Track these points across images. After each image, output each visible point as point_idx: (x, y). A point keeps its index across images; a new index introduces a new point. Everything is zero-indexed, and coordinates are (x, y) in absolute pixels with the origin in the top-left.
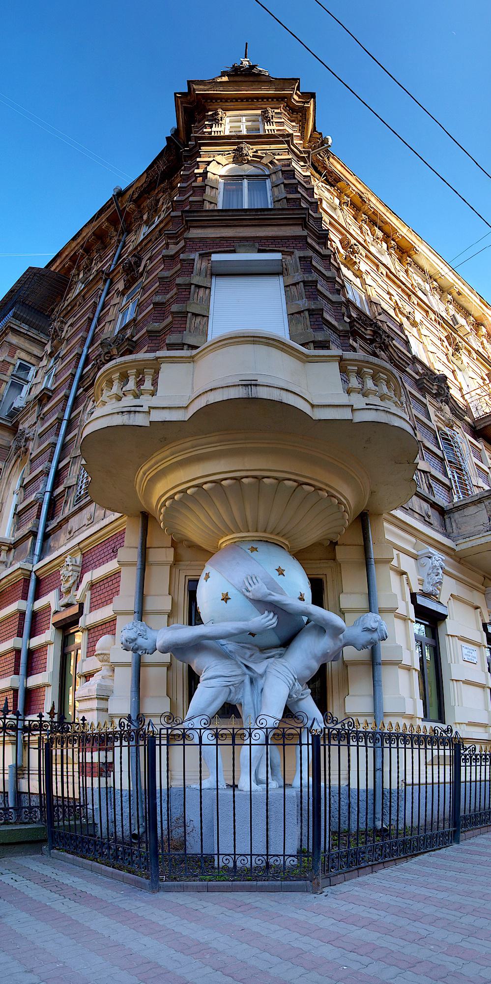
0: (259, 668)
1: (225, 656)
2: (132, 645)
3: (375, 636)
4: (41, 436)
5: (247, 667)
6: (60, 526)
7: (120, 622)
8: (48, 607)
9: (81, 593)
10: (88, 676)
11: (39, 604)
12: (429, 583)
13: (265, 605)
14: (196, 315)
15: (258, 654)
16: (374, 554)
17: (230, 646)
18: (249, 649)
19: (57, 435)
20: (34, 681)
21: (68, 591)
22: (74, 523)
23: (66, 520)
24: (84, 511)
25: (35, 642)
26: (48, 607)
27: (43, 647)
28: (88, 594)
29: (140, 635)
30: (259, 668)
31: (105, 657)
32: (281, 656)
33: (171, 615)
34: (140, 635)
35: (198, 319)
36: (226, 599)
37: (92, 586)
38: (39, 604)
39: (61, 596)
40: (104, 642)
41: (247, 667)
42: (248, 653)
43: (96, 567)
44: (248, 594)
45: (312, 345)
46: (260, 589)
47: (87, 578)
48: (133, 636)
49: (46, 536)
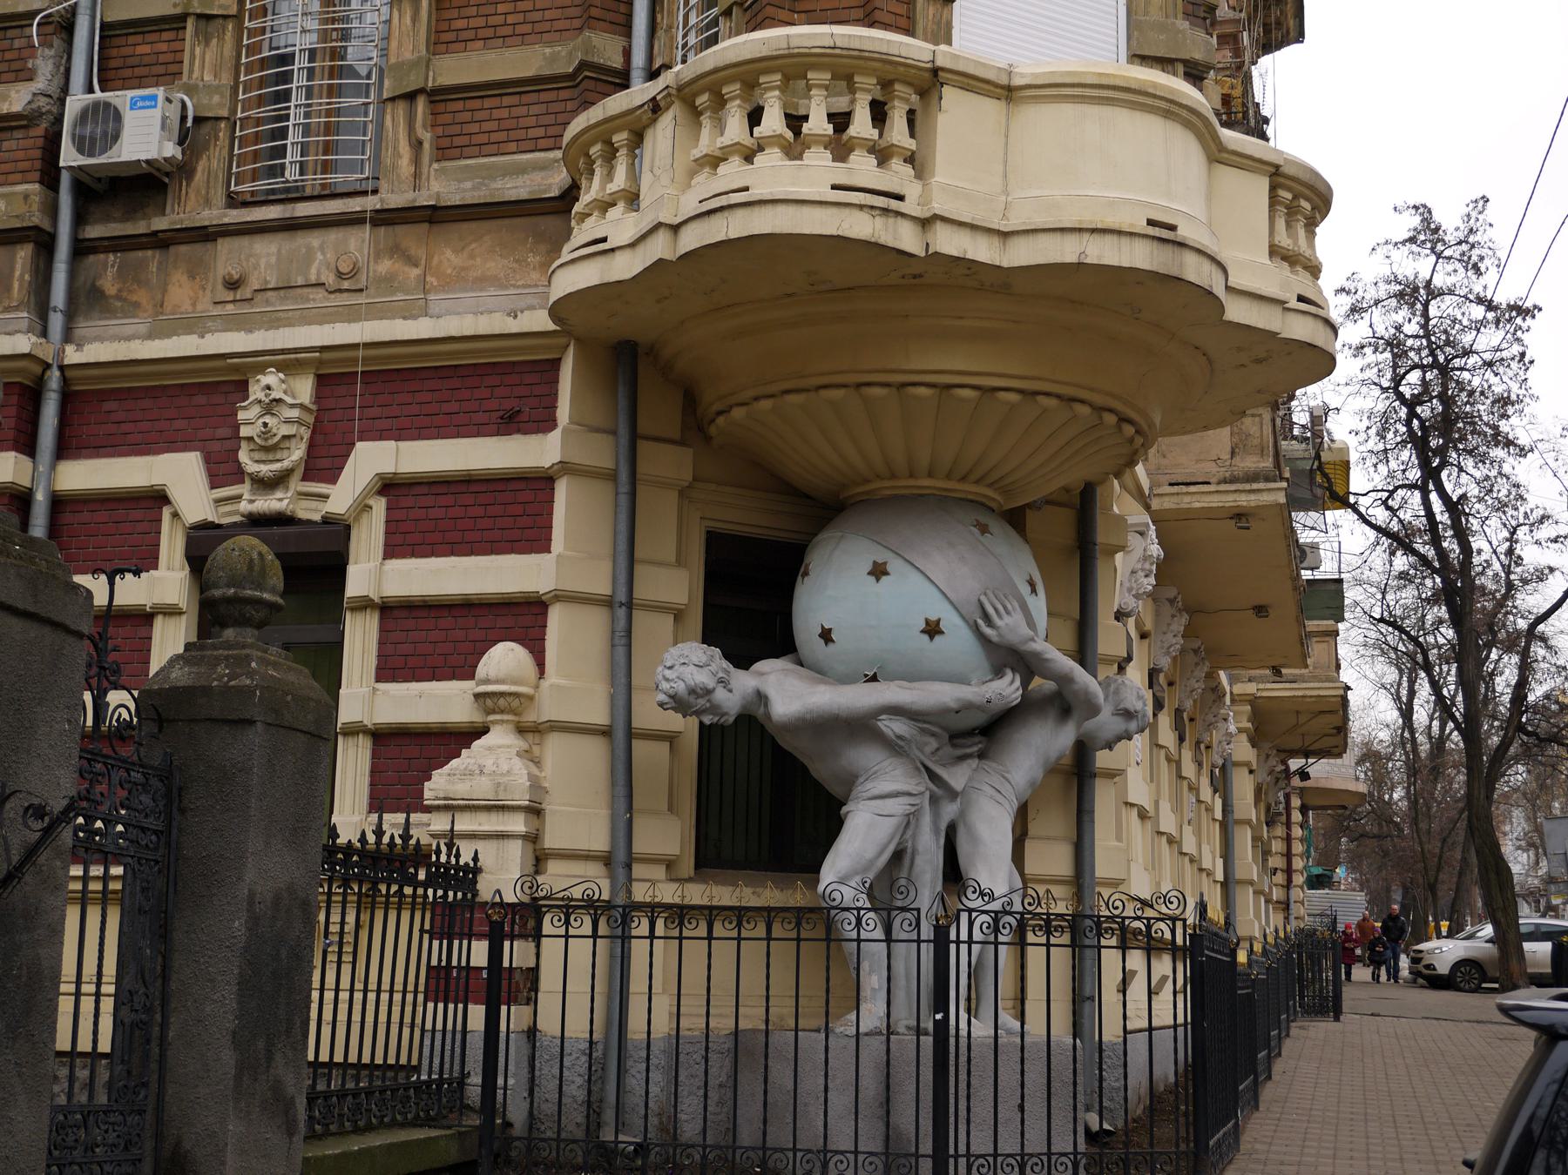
0: (957, 777)
1: (895, 747)
2: (701, 702)
3: (1133, 726)
5: (933, 776)
6: (161, 241)
7: (557, 620)
9: (340, 497)
12: (1130, 590)
13: (1008, 658)
15: (948, 750)
16: (1102, 537)
17: (894, 727)
18: (933, 735)
22: (263, 258)
24: (314, 239)
28: (379, 506)
29: (720, 681)
30: (957, 777)
31: (515, 703)
32: (982, 756)
33: (679, 615)
34: (720, 681)
36: (933, 629)
37: (389, 486)
40: (504, 660)
41: (933, 776)
42: (933, 744)
43: (400, 434)
44: (988, 631)
45: (1180, 68)
46: (1011, 626)
47: (372, 459)
48: (711, 683)
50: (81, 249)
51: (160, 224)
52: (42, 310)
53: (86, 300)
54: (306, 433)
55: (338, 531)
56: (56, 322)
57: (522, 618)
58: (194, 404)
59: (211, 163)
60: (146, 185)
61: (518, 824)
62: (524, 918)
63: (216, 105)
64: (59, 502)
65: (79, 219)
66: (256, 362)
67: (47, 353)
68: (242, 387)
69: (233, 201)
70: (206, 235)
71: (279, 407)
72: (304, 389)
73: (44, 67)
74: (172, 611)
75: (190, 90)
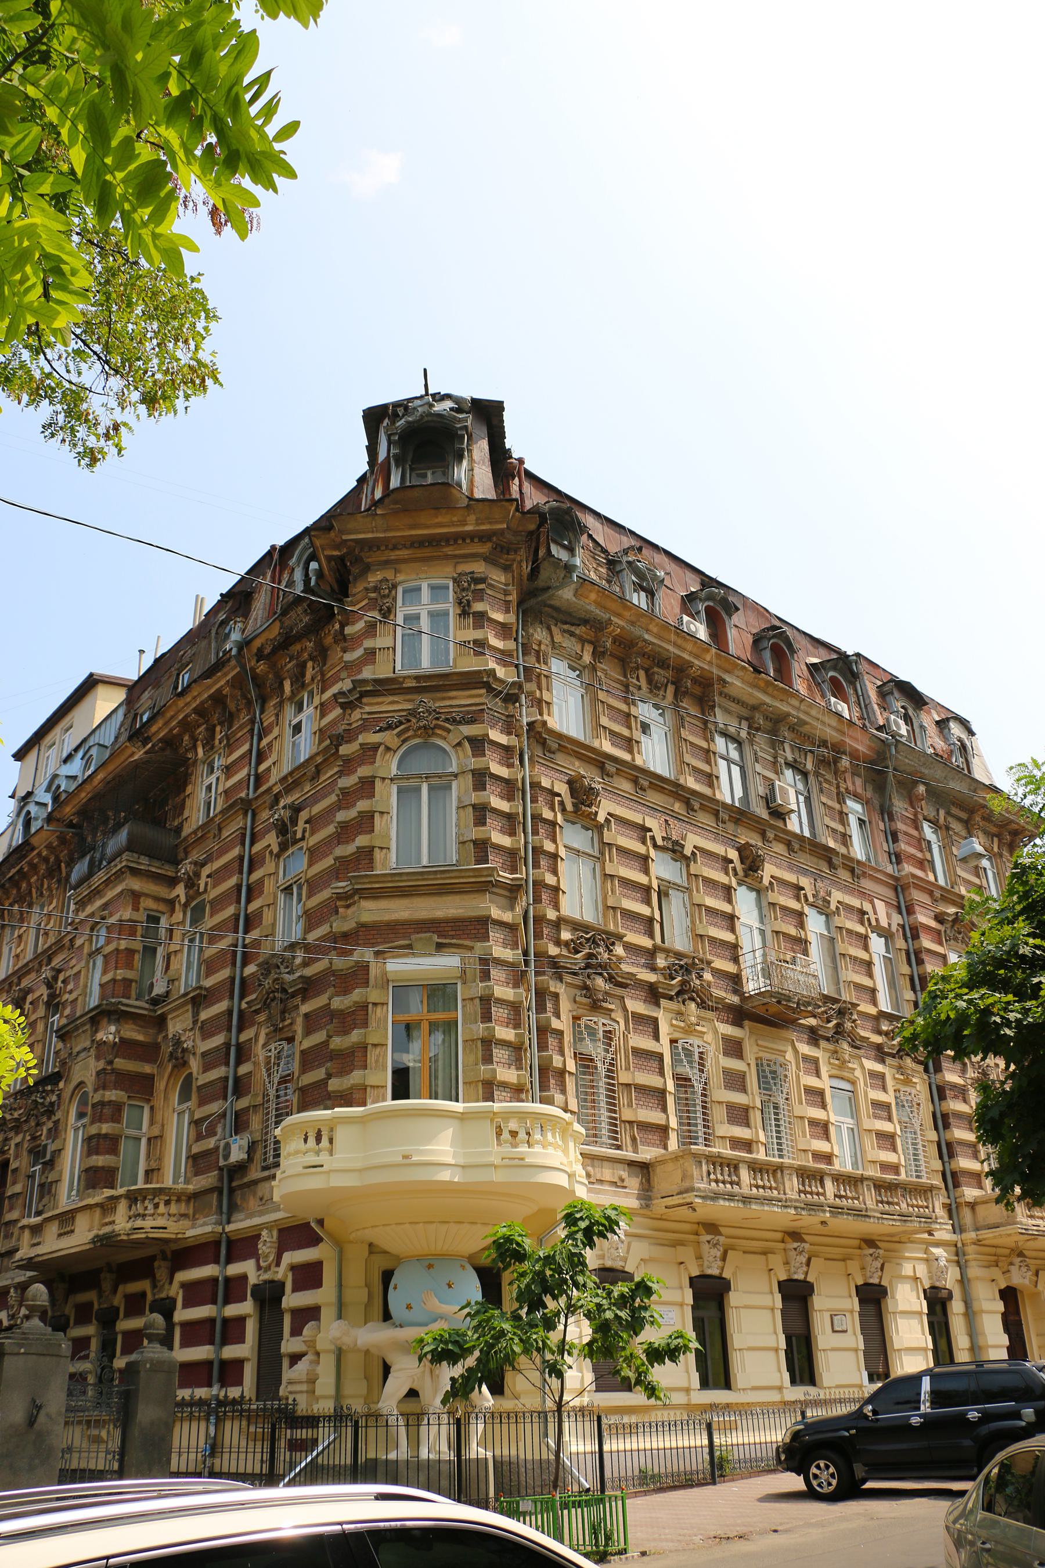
4: (204, 1055)
8: (244, 1277)
9: (281, 1273)
10: (295, 1358)
11: (234, 1269)
14: (375, 1045)
19: (227, 1064)
20: (230, 1352)
21: (268, 1268)
23: (255, 1182)
25: (232, 1310)
26: (244, 1277)
27: (241, 1320)
35: (378, 1050)
36: (409, 1307)
37: (293, 1268)
38: (234, 1269)
39: (259, 1268)
49: (232, 1191)
50: (232, 1191)
51: (246, 1180)
52: (221, 1213)
53: (233, 1208)
54: (274, 1251)
55: (282, 1285)
56: (224, 1217)
57: (311, 1313)
58: (242, 1247)
59: (258, 1156)
60: (241, 1168)
61: (304, 1387)
62: (312, 1421)
63: (257, 1136)
64: (228, 1280)
65: (231, 1180)
66: (261, 1227)
67: (220, 1229)
68: (258, 1236)
69: (264, 1169)
70: (255, 1182)
71: (267, 1244)
72: (275, 1233)
73: (219, 1130)
74: (249, 1316)
75: (251, 1133)
